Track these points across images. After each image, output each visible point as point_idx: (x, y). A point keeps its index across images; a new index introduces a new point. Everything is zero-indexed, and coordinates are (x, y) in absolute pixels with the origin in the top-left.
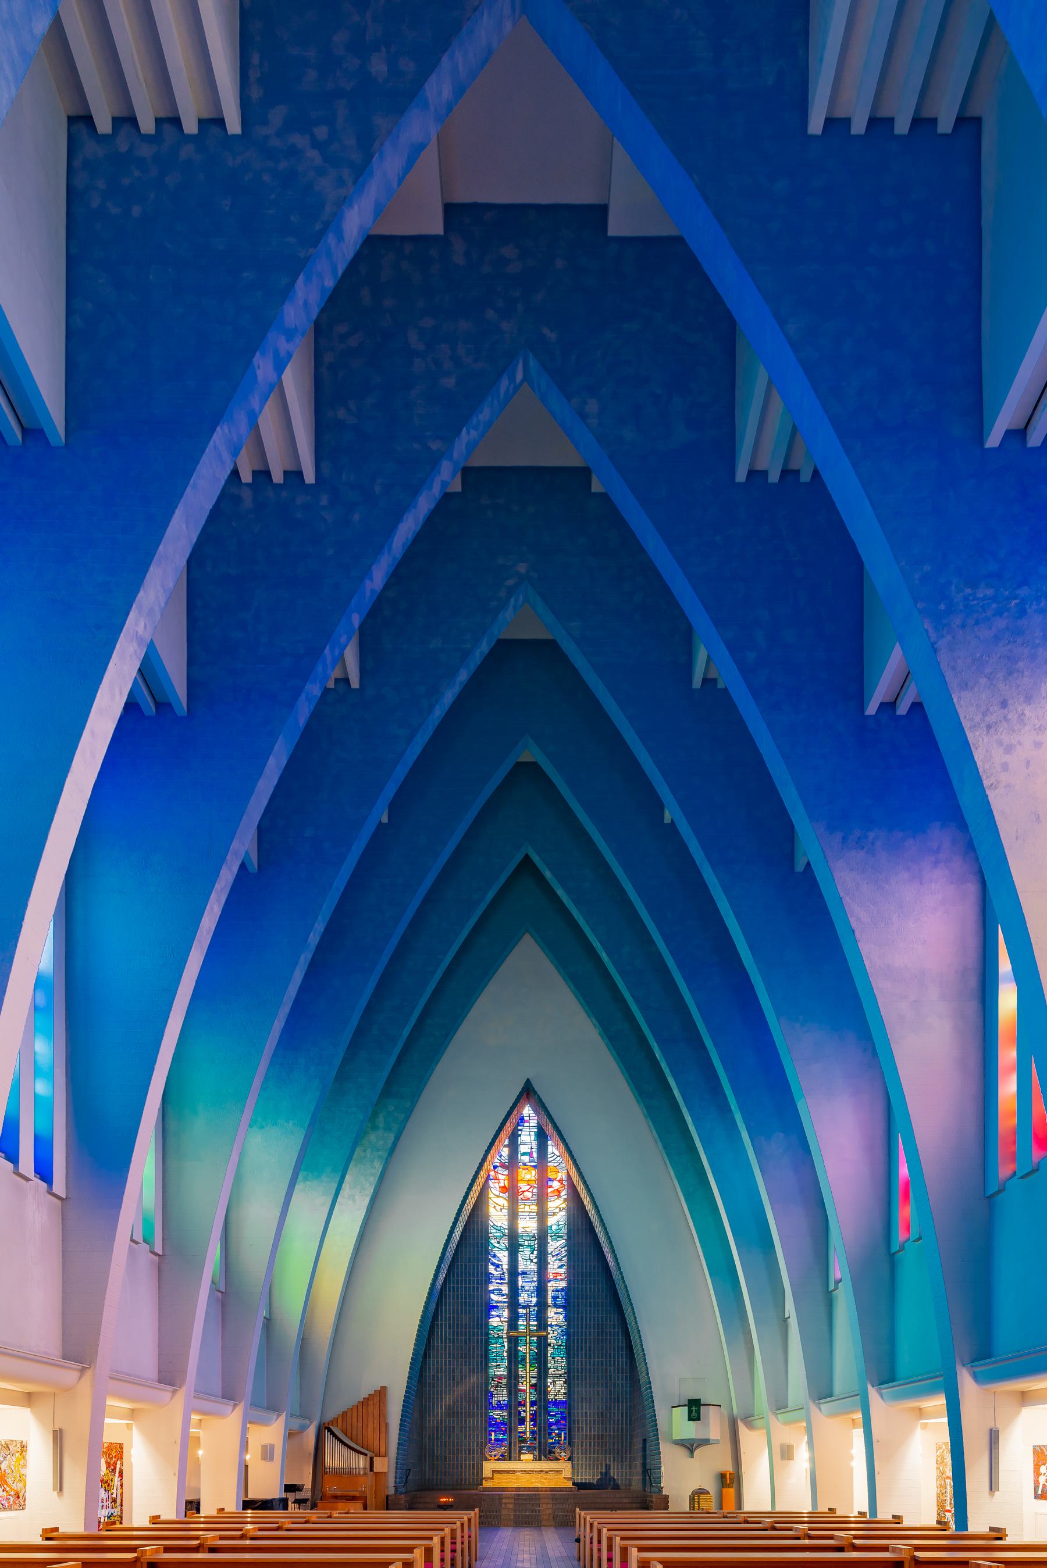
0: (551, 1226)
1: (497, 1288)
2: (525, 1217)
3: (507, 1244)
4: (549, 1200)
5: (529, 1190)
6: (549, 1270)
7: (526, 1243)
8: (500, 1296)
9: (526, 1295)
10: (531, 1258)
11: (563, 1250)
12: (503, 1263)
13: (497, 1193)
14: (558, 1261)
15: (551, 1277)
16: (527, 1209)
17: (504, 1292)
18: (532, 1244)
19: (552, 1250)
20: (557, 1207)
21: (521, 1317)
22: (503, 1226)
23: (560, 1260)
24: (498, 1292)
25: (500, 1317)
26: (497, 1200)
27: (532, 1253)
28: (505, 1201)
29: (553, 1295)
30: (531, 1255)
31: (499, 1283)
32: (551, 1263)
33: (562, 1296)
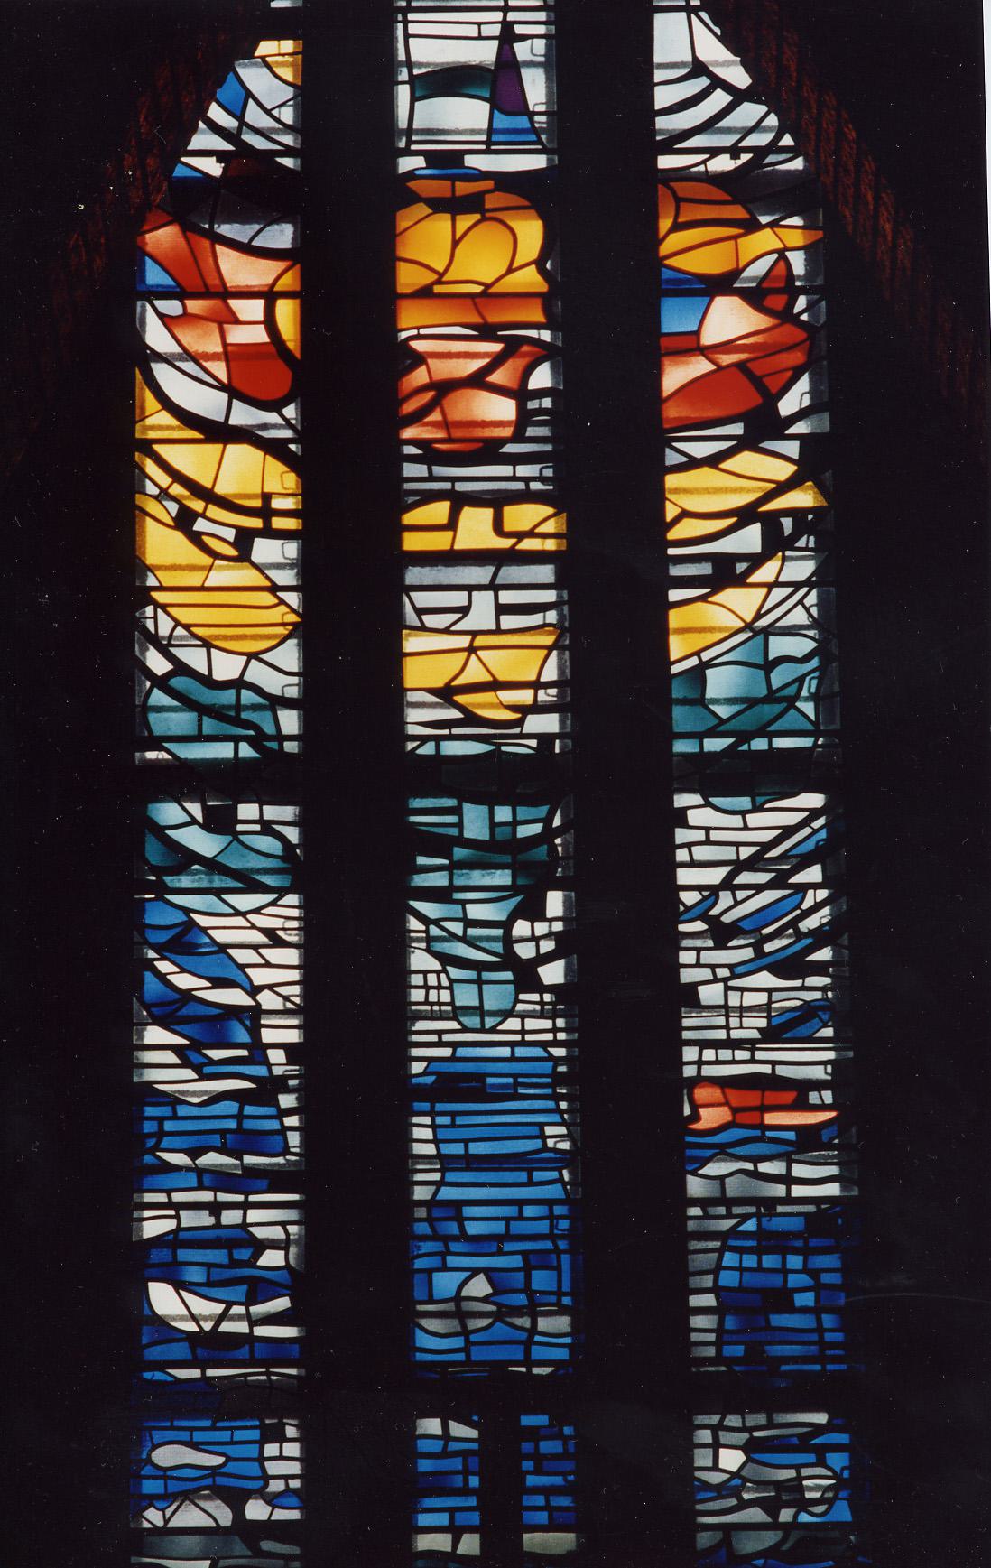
0: (697, 675)
1: (205, 1219)
2: (459, 599)
3: (293, 834)
4: (672, 458)
5: (496, 377)
6: (690, 1054)
7: (475, 822)
8: (240, 1292)
9: (480, 1287)
10: (525, 951)
11: (814, 874)
12: (268, 1000)
13: (208, 403)
14: (765, 979)
15: (711, 1117)
16: (476, 529)
17: (273, 1258)
18: (524, 831)
19: (715, 876)
20: (745, 516)
21: (438, 1485)
22: (257, 673)
23: (791, 966)
24: (219, 1256)
25: (237, 1500)
26: (193, 459)
27: (533, 910)
28: (275, 467)
29: (729, 1279)
30: (521, 928)
31: (220, 1179)
32: (711, 994)
33: (818, 1288)
